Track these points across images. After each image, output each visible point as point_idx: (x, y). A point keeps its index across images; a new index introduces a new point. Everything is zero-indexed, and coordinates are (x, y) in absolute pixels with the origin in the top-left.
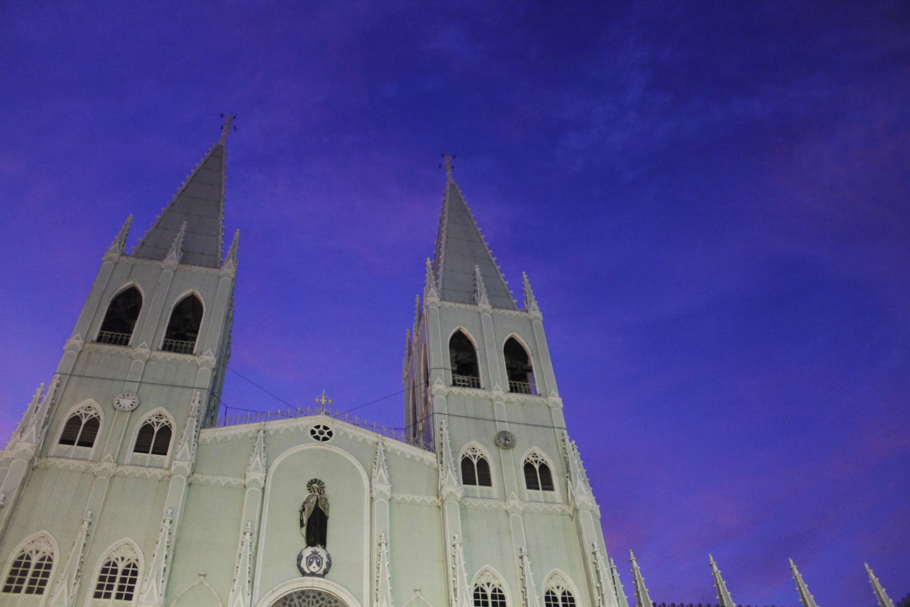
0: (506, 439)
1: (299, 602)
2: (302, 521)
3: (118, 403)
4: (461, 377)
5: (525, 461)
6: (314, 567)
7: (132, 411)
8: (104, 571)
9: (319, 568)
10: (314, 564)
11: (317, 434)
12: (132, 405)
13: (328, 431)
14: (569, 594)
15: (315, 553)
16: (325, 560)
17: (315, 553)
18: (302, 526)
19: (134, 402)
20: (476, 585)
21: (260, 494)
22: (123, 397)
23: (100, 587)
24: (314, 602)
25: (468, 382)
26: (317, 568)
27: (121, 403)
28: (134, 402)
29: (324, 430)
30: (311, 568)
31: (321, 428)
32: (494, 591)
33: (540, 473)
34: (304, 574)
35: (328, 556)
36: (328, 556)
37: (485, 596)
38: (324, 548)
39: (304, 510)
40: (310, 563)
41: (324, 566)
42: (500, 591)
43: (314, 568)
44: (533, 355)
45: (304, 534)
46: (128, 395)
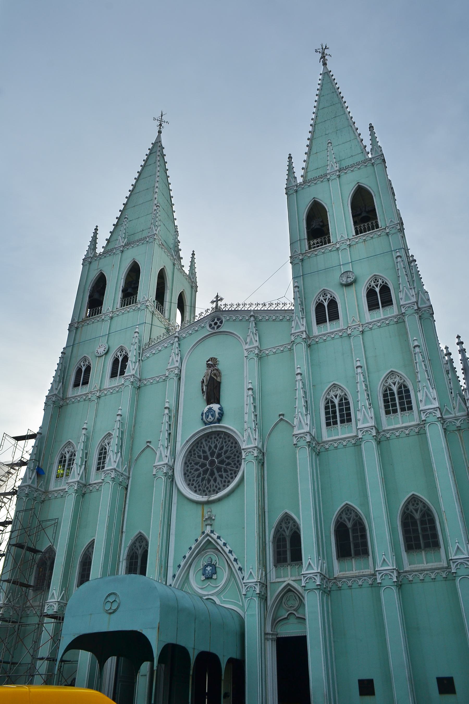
0: (347, 278)
1: (206, 444)
2: (203, 389)
3: (97, 352)
4: (315, 241)
5: (368, 288)
6: (210, 419)
7: (105, 354)
8: (100, 454)
9: (213, 418)
10: (210, 416)
11: (213, 325)
12: (104, 350)
13: (220, 320)
14: (405, 386)
15: (210, 409)
16: (217, 411)
17: (210, 409)
18: (203, 392)
19: (105, 348)
20: (326, 399)
21: (176, 379)
22: (99, 347)
23: (99, 464)
24: (215, 441)
25: (321, 242)
26: (212, 419)
27: (99, 351)
28: (105, 348)
29: (217, 321)
30: (209, 420)
31: (216, 321)
32: (341, 400)
33: (380, 294)
34: (206, 424)
35: (221, 409)
36: (221, 409)
37: (334, 406)
38: (218, 402)
39: (203, 382)
40: (207, 417)
41: (217, 415)
42: (346, 399)
43: (210, 418)
44: (375, 195)
45: (205, 398)
46: (102, 345)
